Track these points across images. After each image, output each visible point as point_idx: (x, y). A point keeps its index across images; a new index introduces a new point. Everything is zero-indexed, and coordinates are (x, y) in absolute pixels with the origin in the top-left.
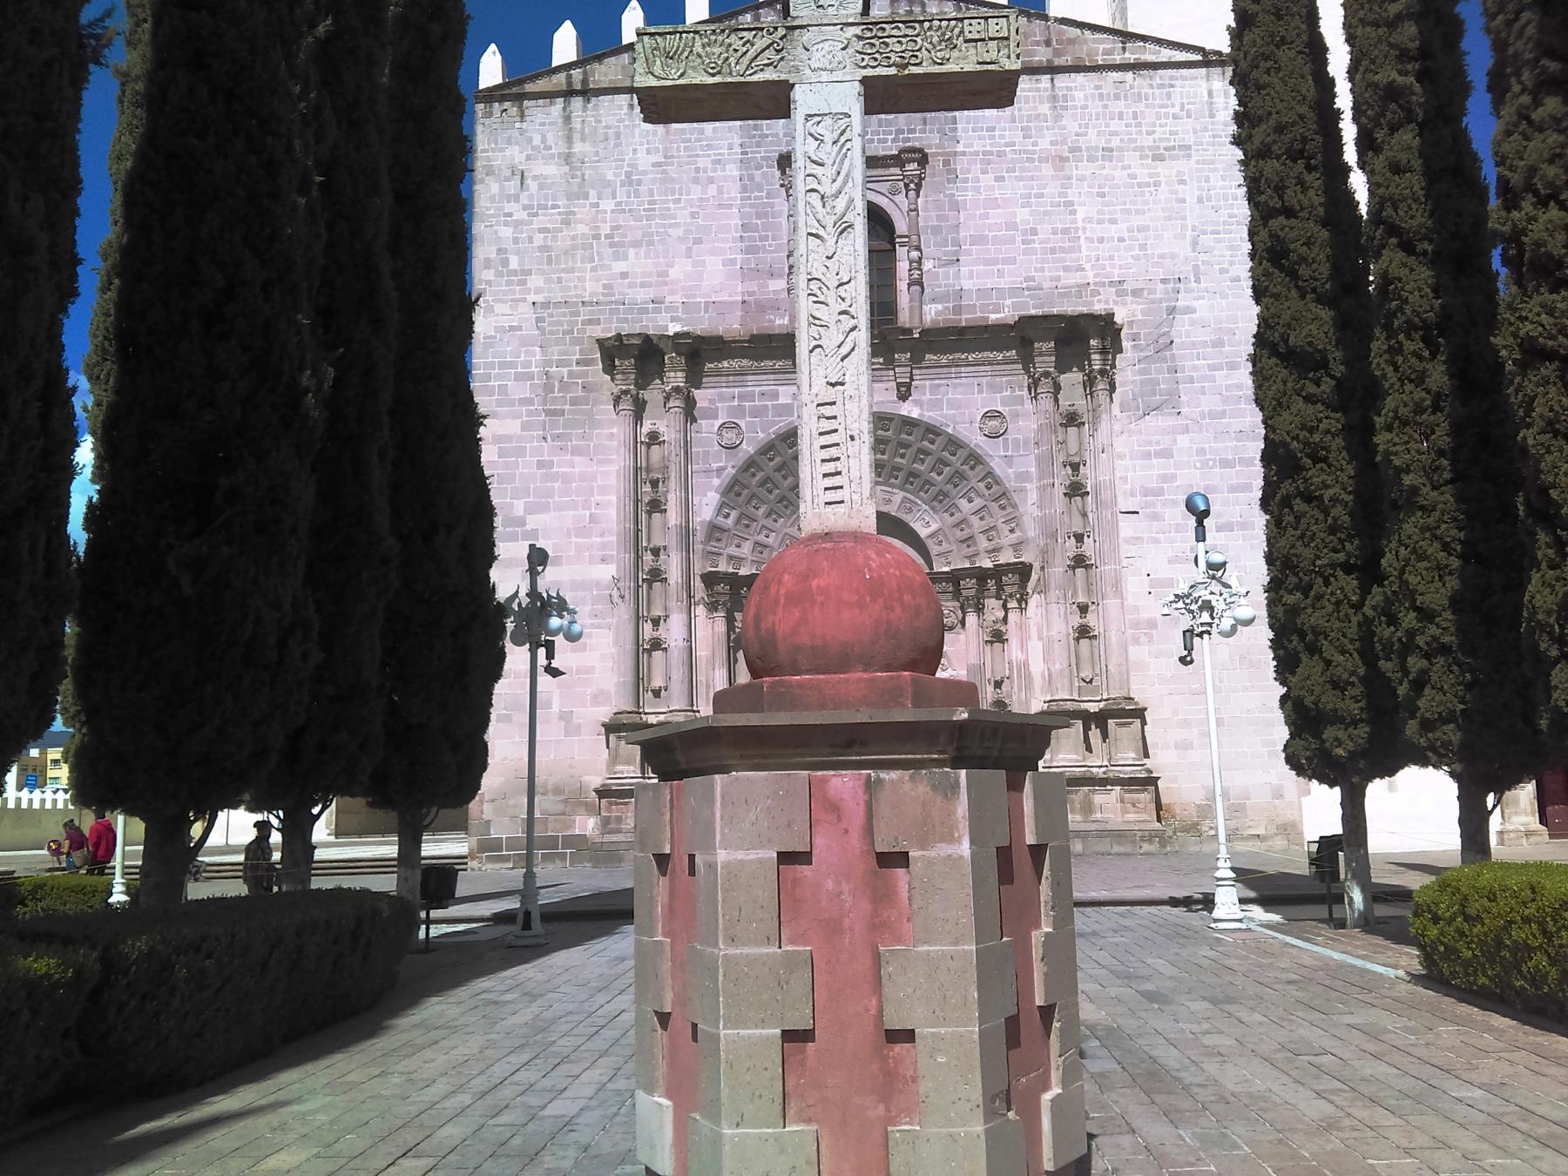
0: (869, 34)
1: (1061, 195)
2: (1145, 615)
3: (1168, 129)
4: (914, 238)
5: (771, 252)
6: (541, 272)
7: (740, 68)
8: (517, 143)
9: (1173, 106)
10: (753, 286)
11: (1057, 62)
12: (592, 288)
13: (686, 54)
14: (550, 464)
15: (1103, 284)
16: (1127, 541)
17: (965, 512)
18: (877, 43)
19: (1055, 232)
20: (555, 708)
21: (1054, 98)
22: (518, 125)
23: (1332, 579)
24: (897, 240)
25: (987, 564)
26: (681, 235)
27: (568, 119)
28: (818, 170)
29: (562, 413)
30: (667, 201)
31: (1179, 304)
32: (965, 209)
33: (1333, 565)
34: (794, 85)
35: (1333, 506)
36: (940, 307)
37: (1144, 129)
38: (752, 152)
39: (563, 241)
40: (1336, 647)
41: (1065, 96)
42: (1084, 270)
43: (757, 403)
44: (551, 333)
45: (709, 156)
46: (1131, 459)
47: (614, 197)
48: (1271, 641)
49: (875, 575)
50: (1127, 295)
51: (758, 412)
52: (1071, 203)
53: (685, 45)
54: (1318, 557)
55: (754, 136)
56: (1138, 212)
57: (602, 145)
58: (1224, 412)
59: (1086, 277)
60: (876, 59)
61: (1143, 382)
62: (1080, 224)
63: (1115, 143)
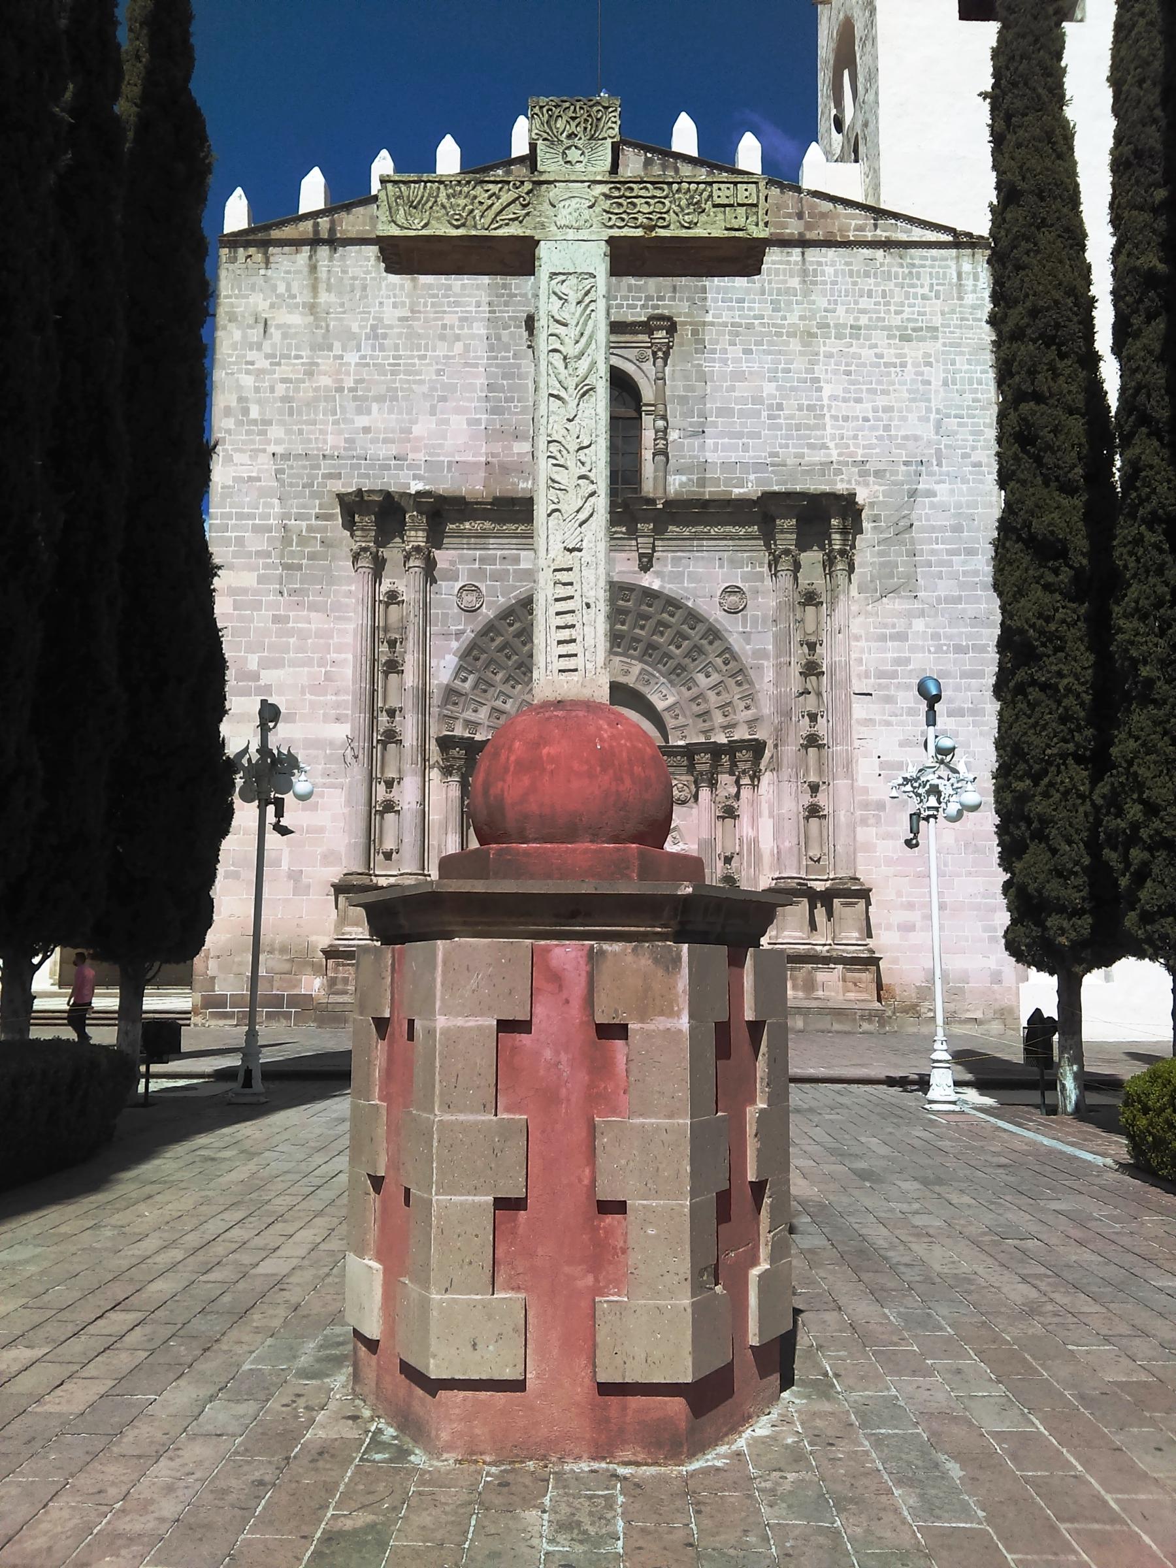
0: (616, 194)
1: (808, 371)
2: (874, 797)
3: (916, 309)
4: (661, 407)
5: (516, 413)
6: (282, 423)
7: (486, 221)
10: (497, 448)
11: (810, 235)
12: (332, 441)
13: (430, 204)
14: (286, 619)
15: (846, 464)
17: (702, 686)
18: (625, 203)
19: (800, 409)
20: (285, 866)
21: (804, 273)
22: (262, 272)
23: (1063, 767)
24: (644, 408)
25: (722, 739)
27: (313, 268)
28: (561, 330)
29: (299, 567)
30: (412, 357)
31: (920, 486)
32: (712, 381)
33: (1064, 756)
34: (539, 241)
35: (1066, 696)
36: (684, 478)
37: (892, 308)
38: (500, 312)
39: (306, 391)
40: (1063, 836)
41: (815, 270)
42: (827, 448)
44: (291, 485)
45: (457, 312)
46: (866, 640)
48: (997, 826)
49: (606, 745)
51: (497, 577)
52: (817, 380)
53: (430, 195)
54: (1049, 746)
56: (884, 392)
58: (960, 597)
59: (829, 455)
60: (623, 220)
61: (883, 565)
62: (826, 402)
63: (864, 320)
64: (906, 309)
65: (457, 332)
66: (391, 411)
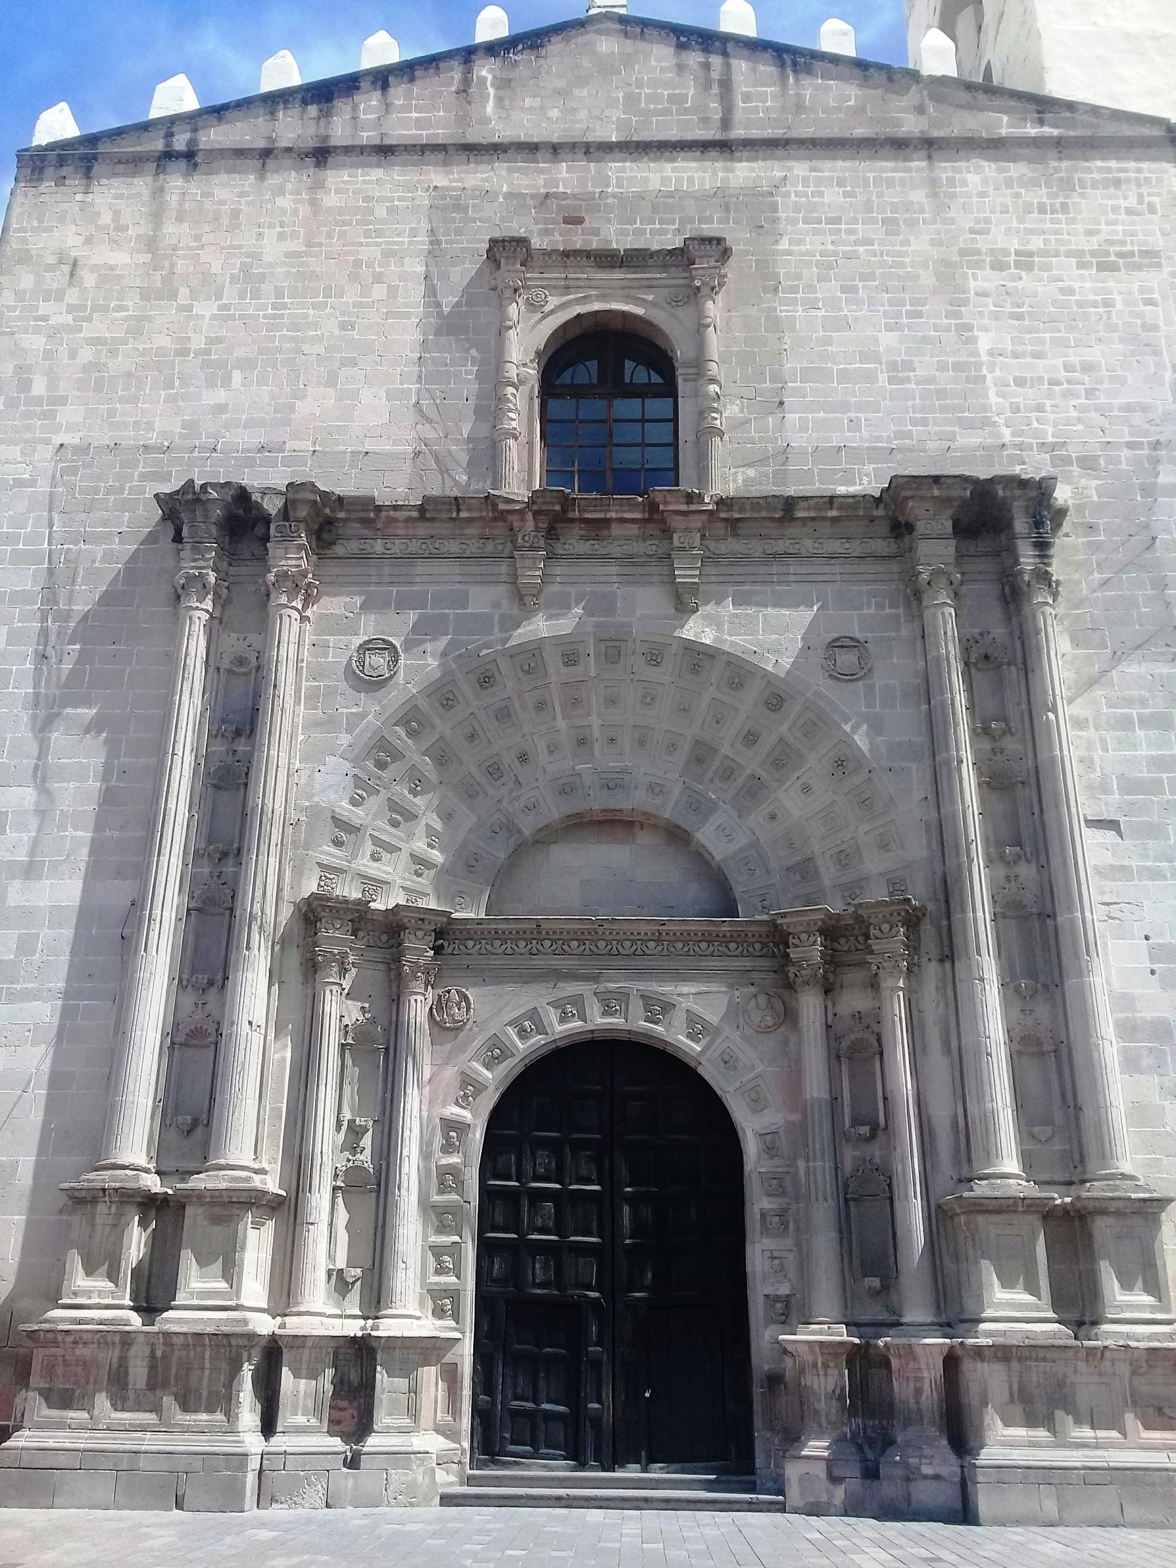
11: (935, 134)
16: (1098, 871)
21: (933, 183)
26: (322, 351)
31: (1162, 479)
32: (794, 330)
36: (751, 472)
37: (1080, 227)
43: (429, 611)
45: (379, 244)
47: (219, 296)
50: (1070, 463)
52: (969, 327)
57: (206, 228)
59: (999, 435)
62: (984, 358)
63: (1036, 243)
64: (1103, 227)
65: (378, 269)
66: (263, 381)
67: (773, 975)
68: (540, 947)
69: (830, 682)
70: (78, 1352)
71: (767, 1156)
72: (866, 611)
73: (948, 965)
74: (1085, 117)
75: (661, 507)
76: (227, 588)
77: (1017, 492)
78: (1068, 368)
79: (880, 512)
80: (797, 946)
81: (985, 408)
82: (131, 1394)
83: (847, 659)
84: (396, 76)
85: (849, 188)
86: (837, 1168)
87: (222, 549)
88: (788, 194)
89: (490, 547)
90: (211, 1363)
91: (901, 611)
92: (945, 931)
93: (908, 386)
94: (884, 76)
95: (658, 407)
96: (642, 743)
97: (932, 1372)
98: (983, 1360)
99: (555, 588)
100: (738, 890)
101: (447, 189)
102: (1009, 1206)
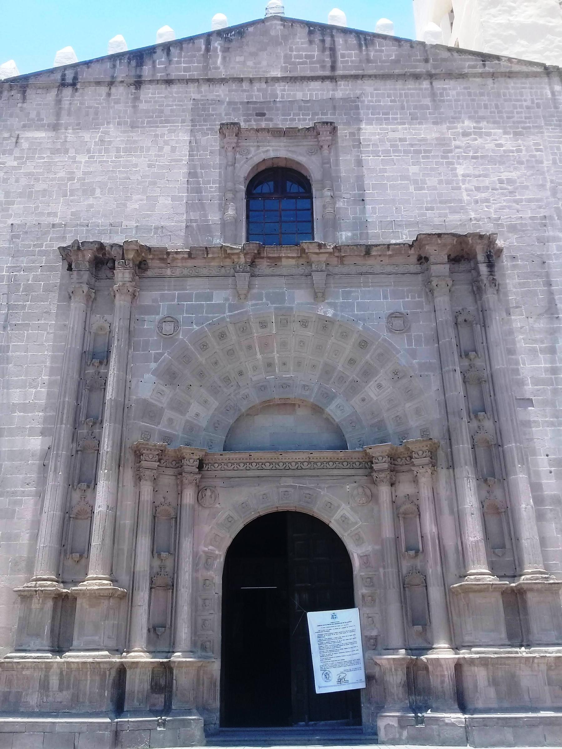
1: (443, 157)
3: (523, 115)
8: (17, 117)
9: (525, 101)
21: (433, 95)
22: (19, 105)
27: (59, 102)
36: (350, 234)
37: (505, 115)
47: (89, 151)
52: (453, 164)
55: (202, 115)
64: (515, 115)
67: (365, 477)
68: (251, 466)
69: (390, 334)
70: (24, 673)
71: (364, 567)
72: (406, 300)
73: (451, 470)
74: (505, 63)
75: (306, 251)
76: (95, 293)
77: (479, 241)
78: (501, 182)
79: (412, 251)
80: (377, 463)
81: (461, 201)
82: (51, 694)
83: (398, 323)
84: (174, 47)
85: (393, 98)
86: (399, 571)
87: (92, 274)
88: (364, 101)
89: (223, 270)
90: (90, 677)
91: (423, 299)
92: (449, 454)
93: (424, 191)
94: (409, 45)
95: (302, 204)
96: (299, 364)
97: (449, 672)
98: (474, 665)
99: (255, 291)
100: (347, 436)
101: (198, 100)
102: (485, 589)
